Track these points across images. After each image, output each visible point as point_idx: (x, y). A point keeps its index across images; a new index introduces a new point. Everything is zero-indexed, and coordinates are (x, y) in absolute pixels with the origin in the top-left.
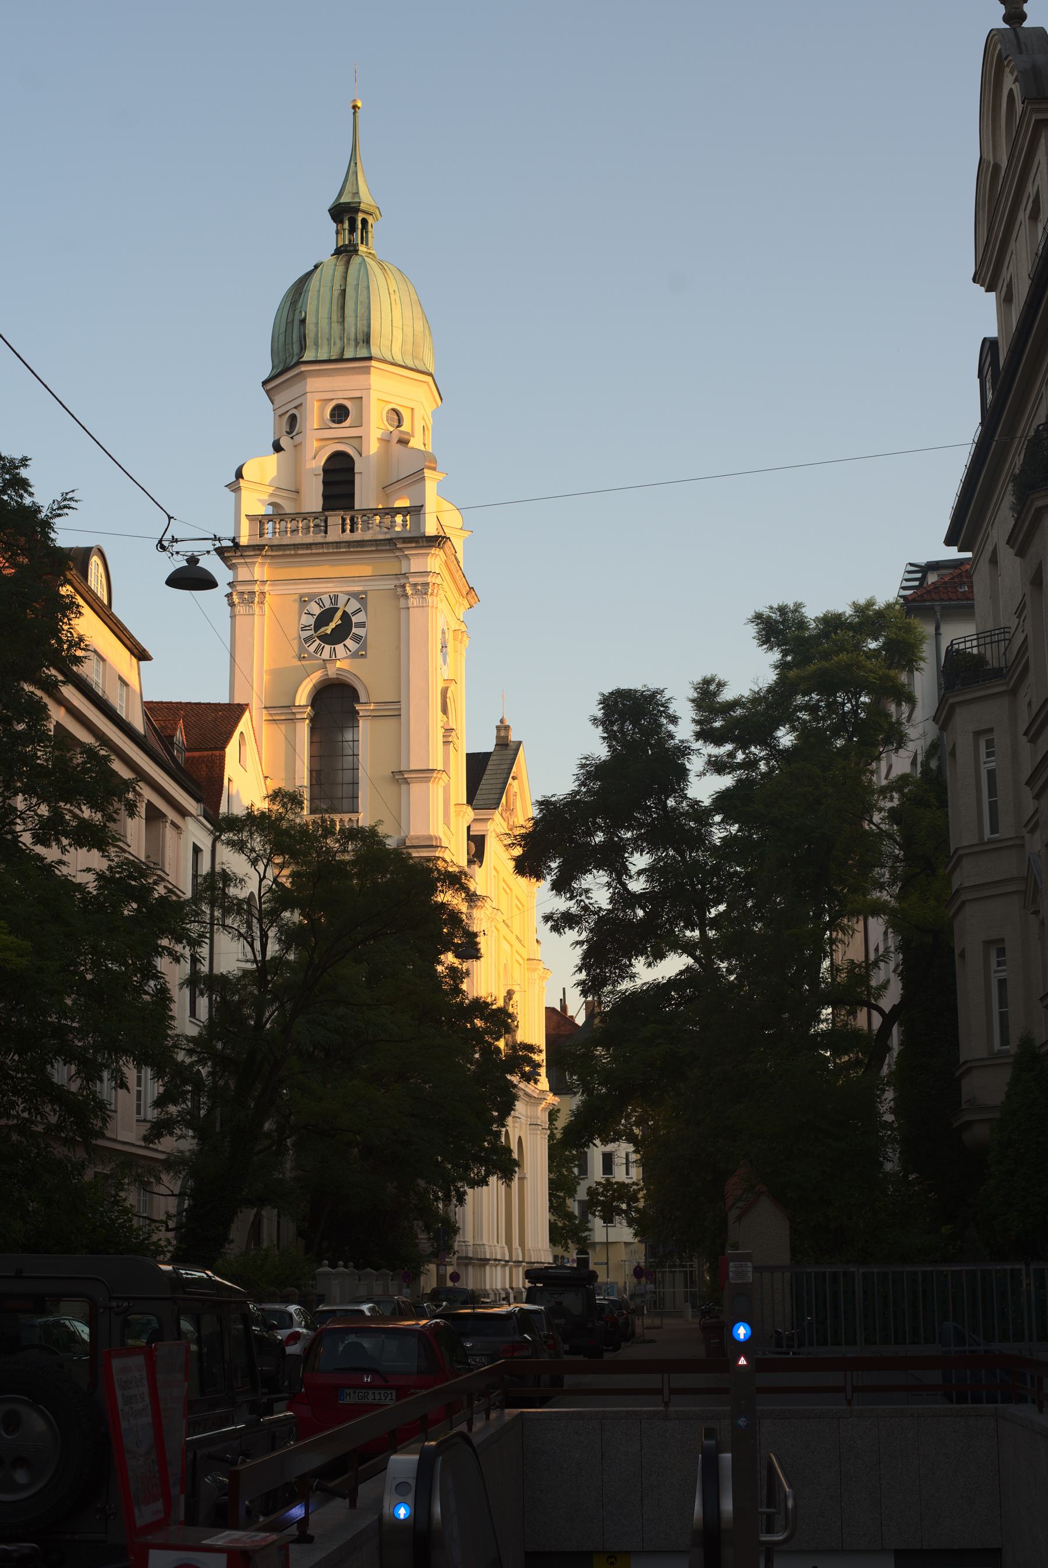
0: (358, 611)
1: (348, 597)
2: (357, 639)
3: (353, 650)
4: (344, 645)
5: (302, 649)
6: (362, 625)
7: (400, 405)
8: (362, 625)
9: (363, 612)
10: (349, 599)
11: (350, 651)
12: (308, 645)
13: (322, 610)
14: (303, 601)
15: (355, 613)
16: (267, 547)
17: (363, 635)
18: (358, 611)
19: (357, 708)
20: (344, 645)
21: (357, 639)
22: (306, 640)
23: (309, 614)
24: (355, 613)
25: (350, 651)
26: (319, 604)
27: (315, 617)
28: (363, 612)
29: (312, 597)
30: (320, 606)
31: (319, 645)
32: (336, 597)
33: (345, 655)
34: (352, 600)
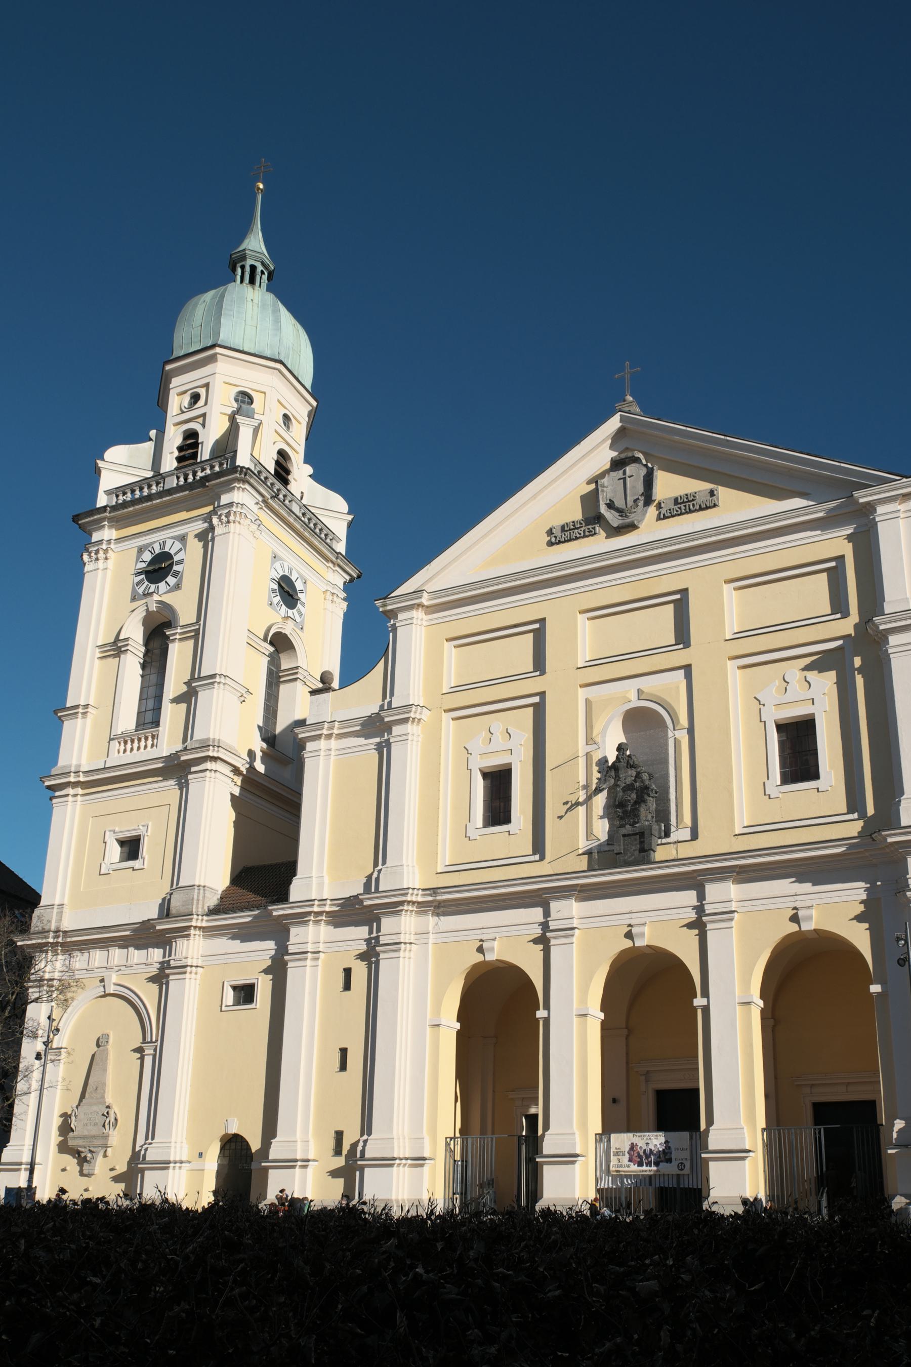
0: (181, 550)
1: (173, 541)
2: (176, 574)
3: (171, 585)
4: (166, 582)
5: (134, 591)
6: (181, 562)
7: (251, 389)
8: (181, 562)
9: (183, 551)
10: (174, 542)
11: (169, 586)
12: (138, 587)
13: (153, 556)
15: (176, 554)
17: (181, 570)
18: (181, 550)
19: (167, 633)
20: (166, 582)
22: (138, 584)
23: (143, 561)
24: (176, 554)
25: (169, 586)
26: (151, 552)
27: (147, 563)
30: (152, 553)
31: (148, 585)
32: (164, 543)
33: (166, 590)
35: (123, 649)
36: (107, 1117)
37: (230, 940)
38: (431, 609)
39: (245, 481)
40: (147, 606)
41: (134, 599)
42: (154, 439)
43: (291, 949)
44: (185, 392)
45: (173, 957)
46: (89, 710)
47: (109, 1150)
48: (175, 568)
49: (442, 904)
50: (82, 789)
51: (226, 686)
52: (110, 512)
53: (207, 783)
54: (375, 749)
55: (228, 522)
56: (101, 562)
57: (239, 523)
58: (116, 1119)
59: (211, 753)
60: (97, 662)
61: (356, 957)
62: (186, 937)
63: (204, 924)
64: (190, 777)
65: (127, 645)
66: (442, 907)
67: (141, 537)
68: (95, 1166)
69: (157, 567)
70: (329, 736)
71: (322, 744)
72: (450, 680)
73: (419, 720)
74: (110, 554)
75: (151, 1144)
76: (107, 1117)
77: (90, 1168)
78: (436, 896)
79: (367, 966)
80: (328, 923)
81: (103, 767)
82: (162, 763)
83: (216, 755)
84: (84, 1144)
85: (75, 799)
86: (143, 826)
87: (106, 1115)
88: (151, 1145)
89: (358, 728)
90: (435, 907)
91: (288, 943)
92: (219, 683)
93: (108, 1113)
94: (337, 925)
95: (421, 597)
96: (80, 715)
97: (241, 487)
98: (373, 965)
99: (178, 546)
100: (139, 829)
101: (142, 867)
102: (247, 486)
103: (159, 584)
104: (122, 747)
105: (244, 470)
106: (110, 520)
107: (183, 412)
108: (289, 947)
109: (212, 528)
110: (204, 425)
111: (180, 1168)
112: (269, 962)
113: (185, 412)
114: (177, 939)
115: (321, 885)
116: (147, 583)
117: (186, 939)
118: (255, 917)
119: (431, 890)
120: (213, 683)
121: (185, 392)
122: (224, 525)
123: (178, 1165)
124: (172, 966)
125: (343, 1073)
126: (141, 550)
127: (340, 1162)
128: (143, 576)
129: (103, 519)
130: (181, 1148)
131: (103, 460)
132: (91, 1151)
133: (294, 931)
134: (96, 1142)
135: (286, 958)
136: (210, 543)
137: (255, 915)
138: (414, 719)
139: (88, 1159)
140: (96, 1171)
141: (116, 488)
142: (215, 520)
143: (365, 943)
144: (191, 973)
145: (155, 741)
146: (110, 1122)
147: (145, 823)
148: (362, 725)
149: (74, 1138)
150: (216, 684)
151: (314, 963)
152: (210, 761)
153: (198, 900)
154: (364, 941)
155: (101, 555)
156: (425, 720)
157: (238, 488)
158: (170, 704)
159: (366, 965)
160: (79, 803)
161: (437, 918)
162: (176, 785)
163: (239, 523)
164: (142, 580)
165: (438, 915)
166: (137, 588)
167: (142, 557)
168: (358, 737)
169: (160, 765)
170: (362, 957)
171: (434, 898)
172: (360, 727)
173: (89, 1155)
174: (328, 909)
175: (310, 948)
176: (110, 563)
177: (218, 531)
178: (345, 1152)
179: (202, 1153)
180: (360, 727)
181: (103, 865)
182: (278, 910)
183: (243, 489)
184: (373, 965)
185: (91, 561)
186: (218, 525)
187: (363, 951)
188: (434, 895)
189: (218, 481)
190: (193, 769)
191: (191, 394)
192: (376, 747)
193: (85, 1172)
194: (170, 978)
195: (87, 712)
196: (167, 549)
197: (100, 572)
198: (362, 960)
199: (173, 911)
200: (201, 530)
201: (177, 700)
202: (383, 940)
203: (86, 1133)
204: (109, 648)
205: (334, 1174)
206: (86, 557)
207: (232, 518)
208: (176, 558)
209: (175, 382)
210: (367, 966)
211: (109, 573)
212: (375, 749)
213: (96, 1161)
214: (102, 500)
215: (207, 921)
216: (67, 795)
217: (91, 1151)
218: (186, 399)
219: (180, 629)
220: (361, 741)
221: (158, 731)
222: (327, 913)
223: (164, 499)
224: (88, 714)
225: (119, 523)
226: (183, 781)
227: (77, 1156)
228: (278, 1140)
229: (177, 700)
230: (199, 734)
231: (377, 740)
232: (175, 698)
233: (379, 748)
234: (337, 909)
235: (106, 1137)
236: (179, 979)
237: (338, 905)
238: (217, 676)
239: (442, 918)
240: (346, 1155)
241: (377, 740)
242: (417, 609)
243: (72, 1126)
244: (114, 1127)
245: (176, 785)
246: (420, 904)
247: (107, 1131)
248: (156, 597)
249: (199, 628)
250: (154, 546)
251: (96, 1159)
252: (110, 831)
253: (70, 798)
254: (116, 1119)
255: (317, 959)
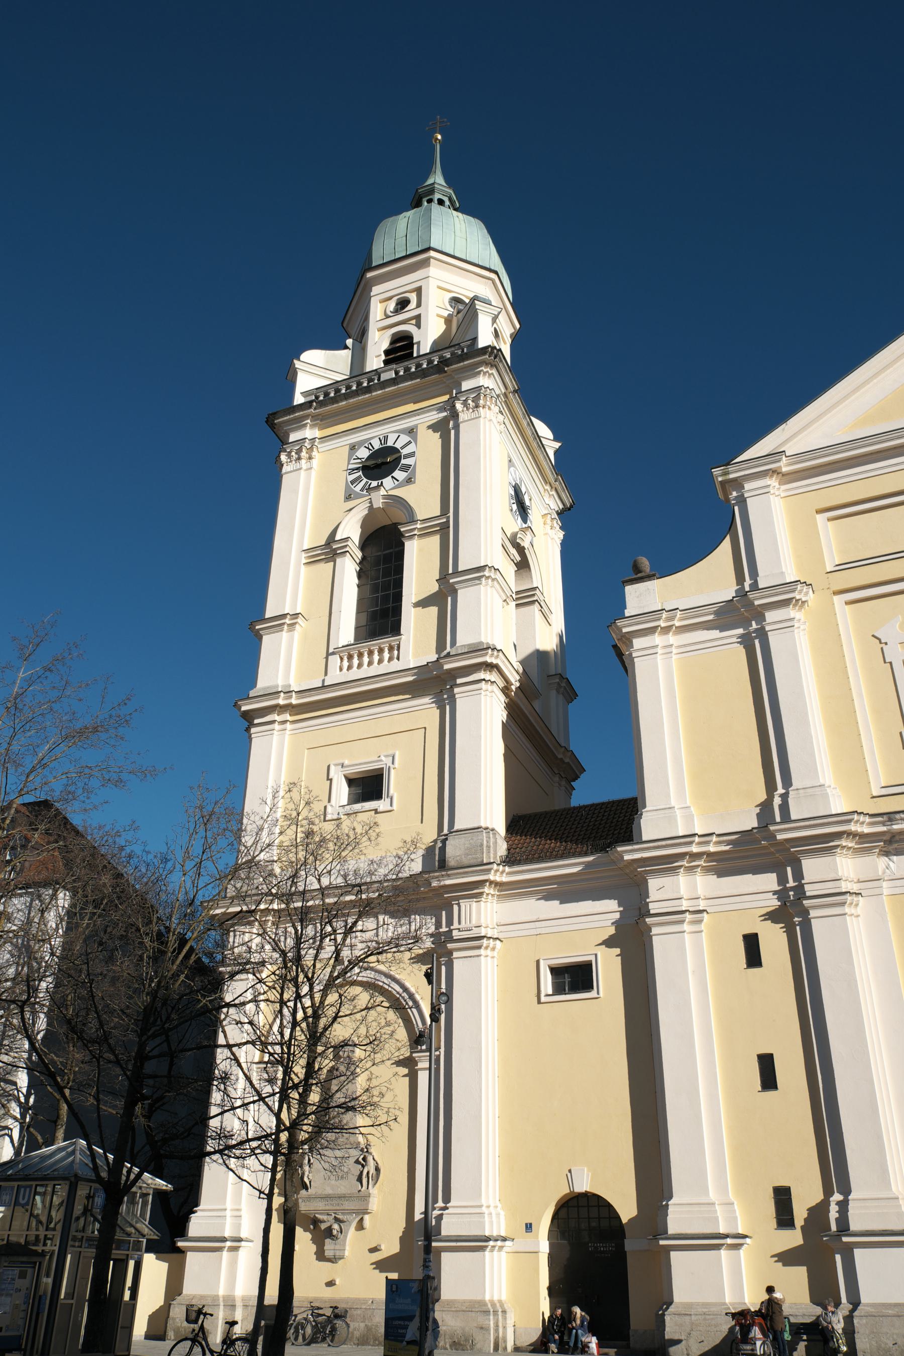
0: (410, 443)
2: (406, 468)
3: (400, 479)
4: (392, 477)
6: (412, 455)
8: (412, 455)
9: (413, 444)
11: (398, 481)
14: (353, 448)
15: (403, 448)
16: (315, 404)
17: (413, 464)
18: (410, 443)
20: (392, 477)
21: (406, 468)
22: (352, 482)
24: (403, 448)
25: (398, 481)
28: (413, 444)
29: (361, 444)
31: (367, 482)
32: (386, 438)
34: (402, 436)
35: (338, 552)
36: (363, 1166)
37: (542, 901)
38: (788, 478)
39: (493, 366)
40: (371, 502)
41: (348, 498)
42: (351, 347)
43: (654, 908)
44: (390, 298)
45: (456, 925)
46: (299, 620)
47: (367, 1218)
48: (403, 461)
49: (897, 838)
50: (290, 715)
51: (495, 583)
52: (315, 409)
53: (483, 697)
54: (738, 642)
55: (477, 406)
56: (303, 461)
57: (489, 408)
58: (377, 1169)
59: (489, 659)
60: (303, 567)
61: (763, 918)
62: (476, 897)
63: (505, 879)
64: (456, 690)
65: (346, 546)
66: (897, 842)
67: (355, 433)
68: (344, 1245)
69: (380, 461)
70: (666, 630)
71: (657, 639)
72: (831, 559)
73: (804, 602)
74: (315, 453)
75: (446, 1208)
76: (363, 1166)
77: (337, 1247)
78: (892, 825)
79: (785, 929)
80: (707, 870)
81: (321, 685)
82: (413, 676)
83: (495, 661)
84: (327, 1208)
85: (282, 727)
86: (386, 756)
87: (362, 1162)
88: (447, 1211)
89: (711, 617)
90: (885, 842)
91: (648, 900)
92: (488, 578)
93: (364, 1159)
94: (721, 873)
95: (779, 461)
96: (286, 627)
97: (487, 372)
98: (798, 928)
99: (404, 439)
100: (381, 761)
101: (389, 808)
102: (494, 371)
103: (383, 480)
104: (346, 664)
105: (495, 351)
106: (314, 417)
107: (387, 317)
108: (651, 906)
109: (455, 415)
110: (418, 325)
111: (501, 1247)
112: (612, 931)
113: (391, 317)
114: (460, 901)
115: (689, 818)
116: (365, 480)
117: (475, 900)
118: (588, 865)
119: (885, 816)
120: (479, 578)
121: (390, 298)
122: (471, 410)
123: (499, 1243)
124: (455, 938)
125: (771, 1094)
126: (353, 448)
127: (793, 1238)
128: (361, 473)
129: (306, 417)
130: (498, 1215)
131: (299, 360)
132: (337, 1220)
133: (654, 884)
134: (348, 1205)
135: (648, 920)
136: (453, 432)
137: (588, 862)
138: (797, 601)
139: (335, 1232)
140: (347, 1253)
141: (316, 389)
142: (459, 406)
143: (776, 897)
144: (486, 948)
145: (396, 652)
146: (368, 1173)
147: (391, 752)
148: (716, 613)
149: (309, 1198)
150: (483, 579)
151: (695, 928)
152: (485, 670)
153: (488, 847)
154: (773, 894)
155: (304, 454)
156: (810, 605)
157: (485, 373)
158: (413, 609)
159: (781, 928)
160: (288, 732)
161: (886, 858)
162: (432, 703)
163: (489, 408)
164: (360, 477)
165: (887, 854)
166: (352, 487)
167: (356, 454)
168: (708, 629)
169: (411, 679)
170: (772, 916)
171: (889, 827)
172: (713, 616)
173: (336, 1227)
174: (712, 848)
175: (685, 905)
176: (315, 462)
177: (462, 417)
178: (799, 1221)
179: (531, 1224)
180: (713, 616)
181: (329, 809)
182: (629, 853)
183: (490, 375)
184: (798, 928)
185: (291, 461)
186: (463, 411)
187: (774, 908)
188: (889, 823)
189: (462, 364)
190: (459, 681)
191: (398, 299)
192: (739, 640)
193: (328, 1253)
194: (454, 956)
195: (295, 623)
196: (390, 443)
197: (302, 472)
198: (775, 921)
199: (451, 861)
200: (436, 420)
201: (423, 603)
202: (810, 890)
203: (329, 1191)
204: (319, 552)
205: (787, 1258)
206: (283, 457)
207: (481, 402)
208: (404, 452)
209: (375, 290)
210: (785, 929)
211: (314, 473)
212: (738, 642)
213: (346, 1237)
214: (299, 399)
215: (509, 874)
216: (273, 722)
217: (337, 1220)
218: (392, 305)
219: (420, 524)
220: (715, 634)
221: (399, 640)
222: (709, 855)
223: (387, 390)
224: (297, 626)
225: (323, 421)
226: (445, 696)
227: (312, 1227)
228: (677, 1202)
229: (423, 603)
230: (464, 638)
231: (740, 631)
232: (419, 601)
233: (746, 642)
234: (727, 848)
235: (366, 1198)
236: (471, 957)
237: (729, 843)
238: (487, 568)
239: (895, 858)
240: (802, 1227)
241: (740, 631)
242: (772, 476)
243: (306, 1179)
244: (374, 1181)
245: (432, 703)
246: (862, 837)
247: (364, 1188)
248: (382, 492)
249: (448, 521)
250: (372, 442)
251: (347, 1233)
252: (336, 765)
253: (276, 726)
254: (377, 1169)
255: (700, 921)
